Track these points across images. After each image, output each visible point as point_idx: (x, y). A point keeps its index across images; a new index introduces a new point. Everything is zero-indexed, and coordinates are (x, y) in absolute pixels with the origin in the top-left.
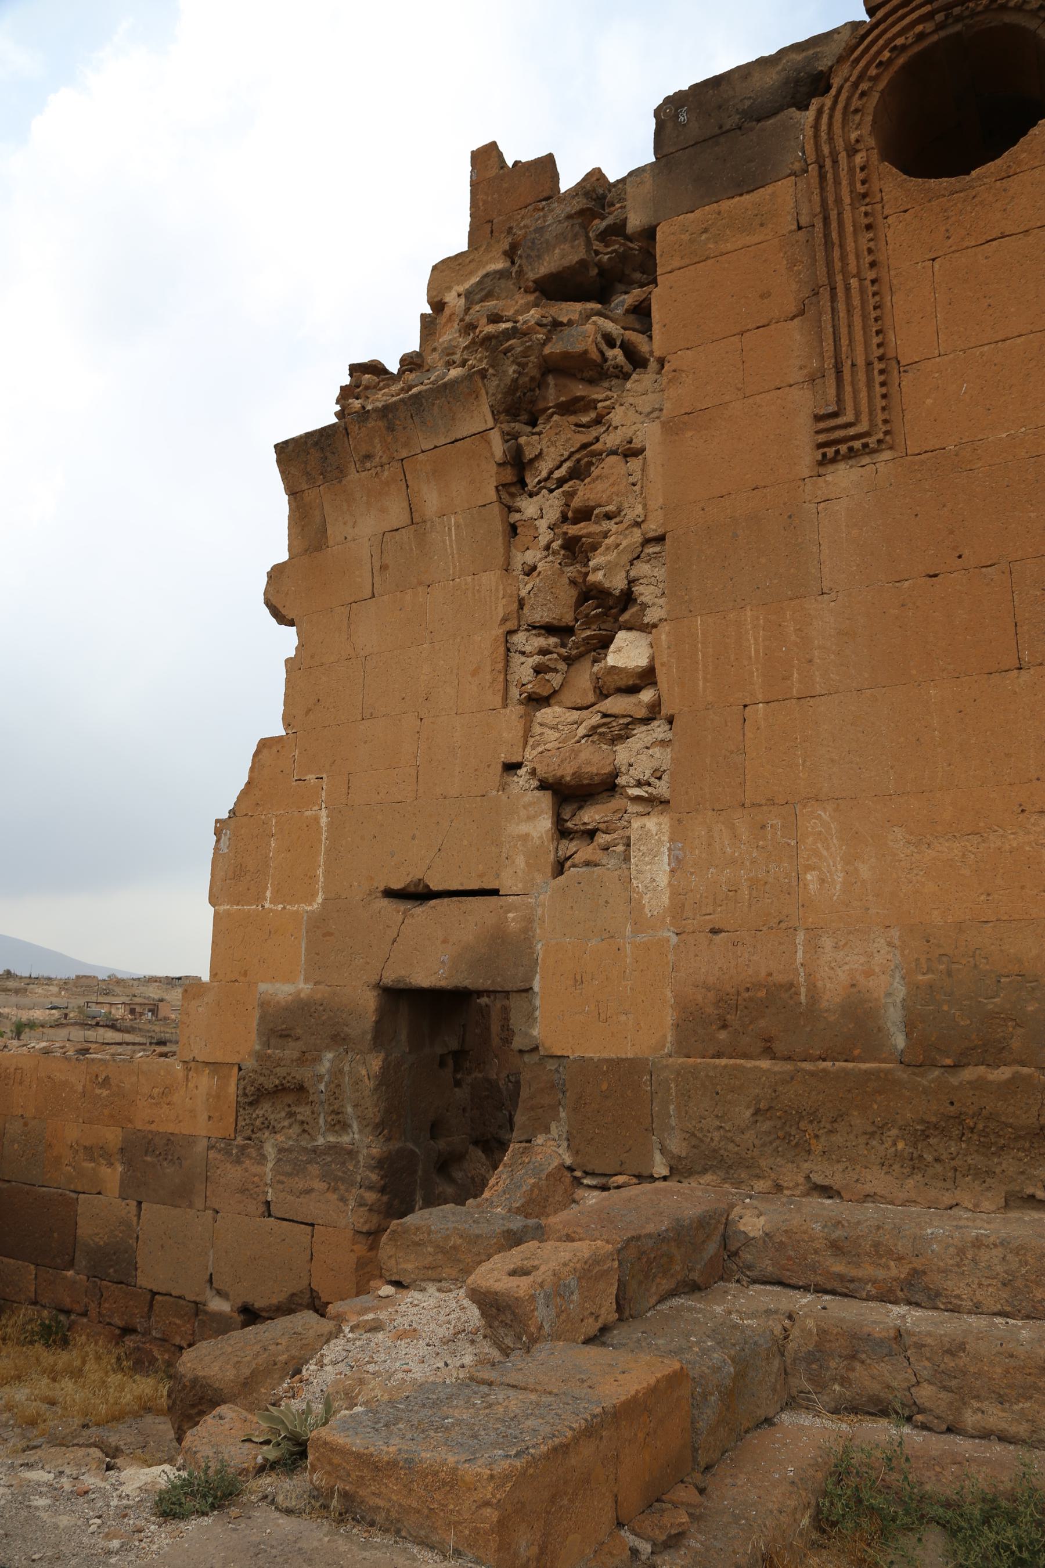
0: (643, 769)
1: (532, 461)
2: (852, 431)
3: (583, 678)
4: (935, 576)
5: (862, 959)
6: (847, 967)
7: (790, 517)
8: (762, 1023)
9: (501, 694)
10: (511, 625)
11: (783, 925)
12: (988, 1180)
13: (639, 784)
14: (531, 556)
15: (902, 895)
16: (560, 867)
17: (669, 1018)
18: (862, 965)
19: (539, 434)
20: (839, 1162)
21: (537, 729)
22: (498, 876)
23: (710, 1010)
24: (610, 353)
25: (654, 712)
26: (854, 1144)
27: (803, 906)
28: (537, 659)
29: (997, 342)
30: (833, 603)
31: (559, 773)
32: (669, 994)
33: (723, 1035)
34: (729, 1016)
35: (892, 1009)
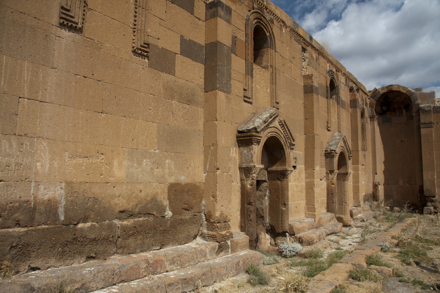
4: (86, 77)
5: (53, 193)
6: (47, 195)
7: (46, 36)
8: (16, 215)
11: (27, 180)
12: (82, 254)
15: (66, 173)
18: (52, 195)
20: (40, 258)
26: (46, 252)
27: (35, 174)
29: (111, 18)
30: (56, 73)
34: (2, 213)
35: (60, 208)
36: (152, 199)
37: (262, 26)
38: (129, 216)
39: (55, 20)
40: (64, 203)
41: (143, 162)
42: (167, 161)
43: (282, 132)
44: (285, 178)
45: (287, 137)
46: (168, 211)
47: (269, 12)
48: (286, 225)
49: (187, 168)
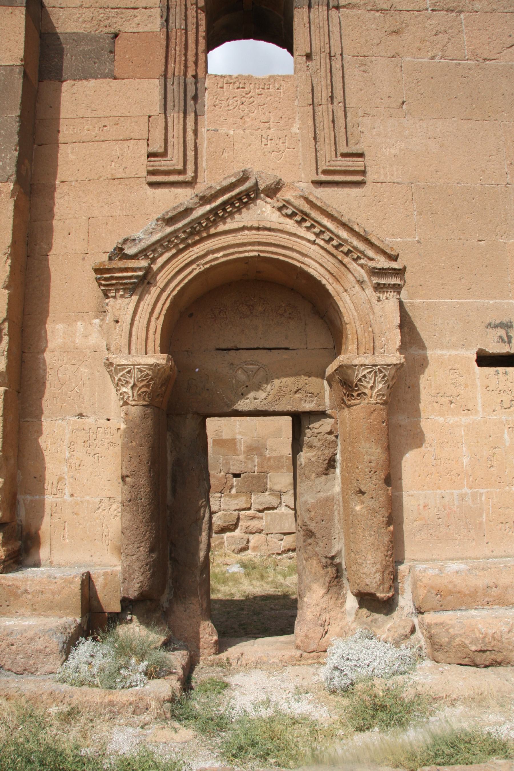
43: (312, 237)
44: (355, 394)
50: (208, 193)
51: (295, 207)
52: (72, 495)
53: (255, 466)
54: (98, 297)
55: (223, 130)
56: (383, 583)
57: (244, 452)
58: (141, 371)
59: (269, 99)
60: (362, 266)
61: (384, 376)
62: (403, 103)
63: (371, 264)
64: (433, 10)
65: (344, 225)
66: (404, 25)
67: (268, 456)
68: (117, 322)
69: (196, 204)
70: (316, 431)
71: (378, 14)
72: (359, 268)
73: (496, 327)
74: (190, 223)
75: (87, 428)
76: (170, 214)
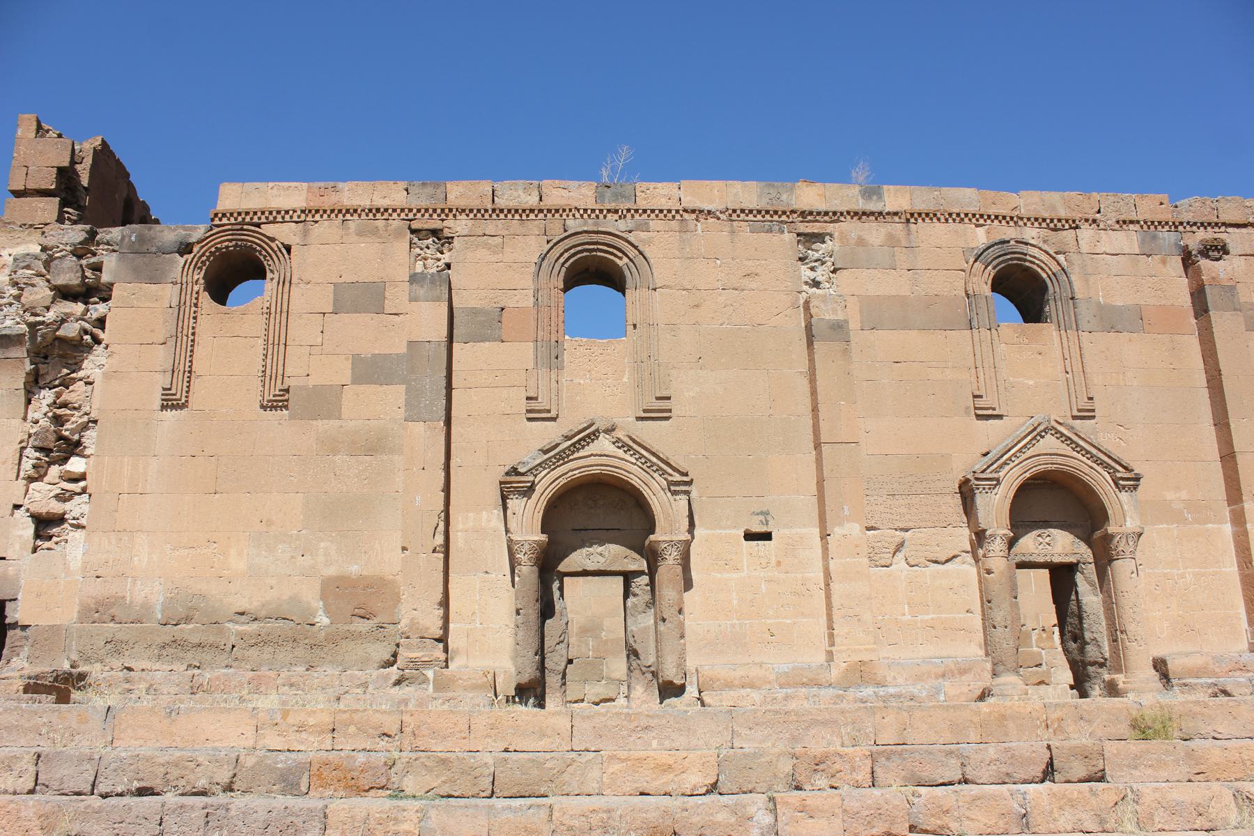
0: (76, 513)
1: (43, 375)
2: (174, 397)
3: (55, 470)
8: (112, 610)
9: (16, 474)
10: (24, 444)
13: (74, 519)
14: (37, 416)
16: (35, 550)
17: (76, 608)
19: (48, 363)
21: (30, 491)
22: (6, 552)
23: (92, 606)
24: (85, 337)
25: (84, 491)
28: (35, 461)
31: (40, 511)
32: (77, 600)
33: (97, 615)
36: (291, 598)
37: (599, 254)
38: (252, 619)
39: (158, 403)
40: (162, 601)
41: (277, 548)
42: (322, 545)
43: (634, 461)
45: (653, 470)
46: (321, 617)
47: (625, 216)
48: (667, 666)
49: (365, 552)
50: (570, 434)
51: (623, 442)
52: (481, 624)
53: (589, 650)
54: (496, 495)
55: (576, 381)
56: (677, 674)
57: (577, 634)
58: (530, 545)
59: (608, 357)
60: (665, 479)
61: (678, 547)
62: (700, 358)
63: (670, 478)
64: (722, 289)
65: (654, 454)
66: (702, 301)
67: (605, 638)
68: (514, 514)
69: (562, 440)
70: (638, 584)
71: (684, 292)
72: (663, 480)
73: (758, 514)
74: (559, 453)
75: (490, 581)
76: (547, 448)
